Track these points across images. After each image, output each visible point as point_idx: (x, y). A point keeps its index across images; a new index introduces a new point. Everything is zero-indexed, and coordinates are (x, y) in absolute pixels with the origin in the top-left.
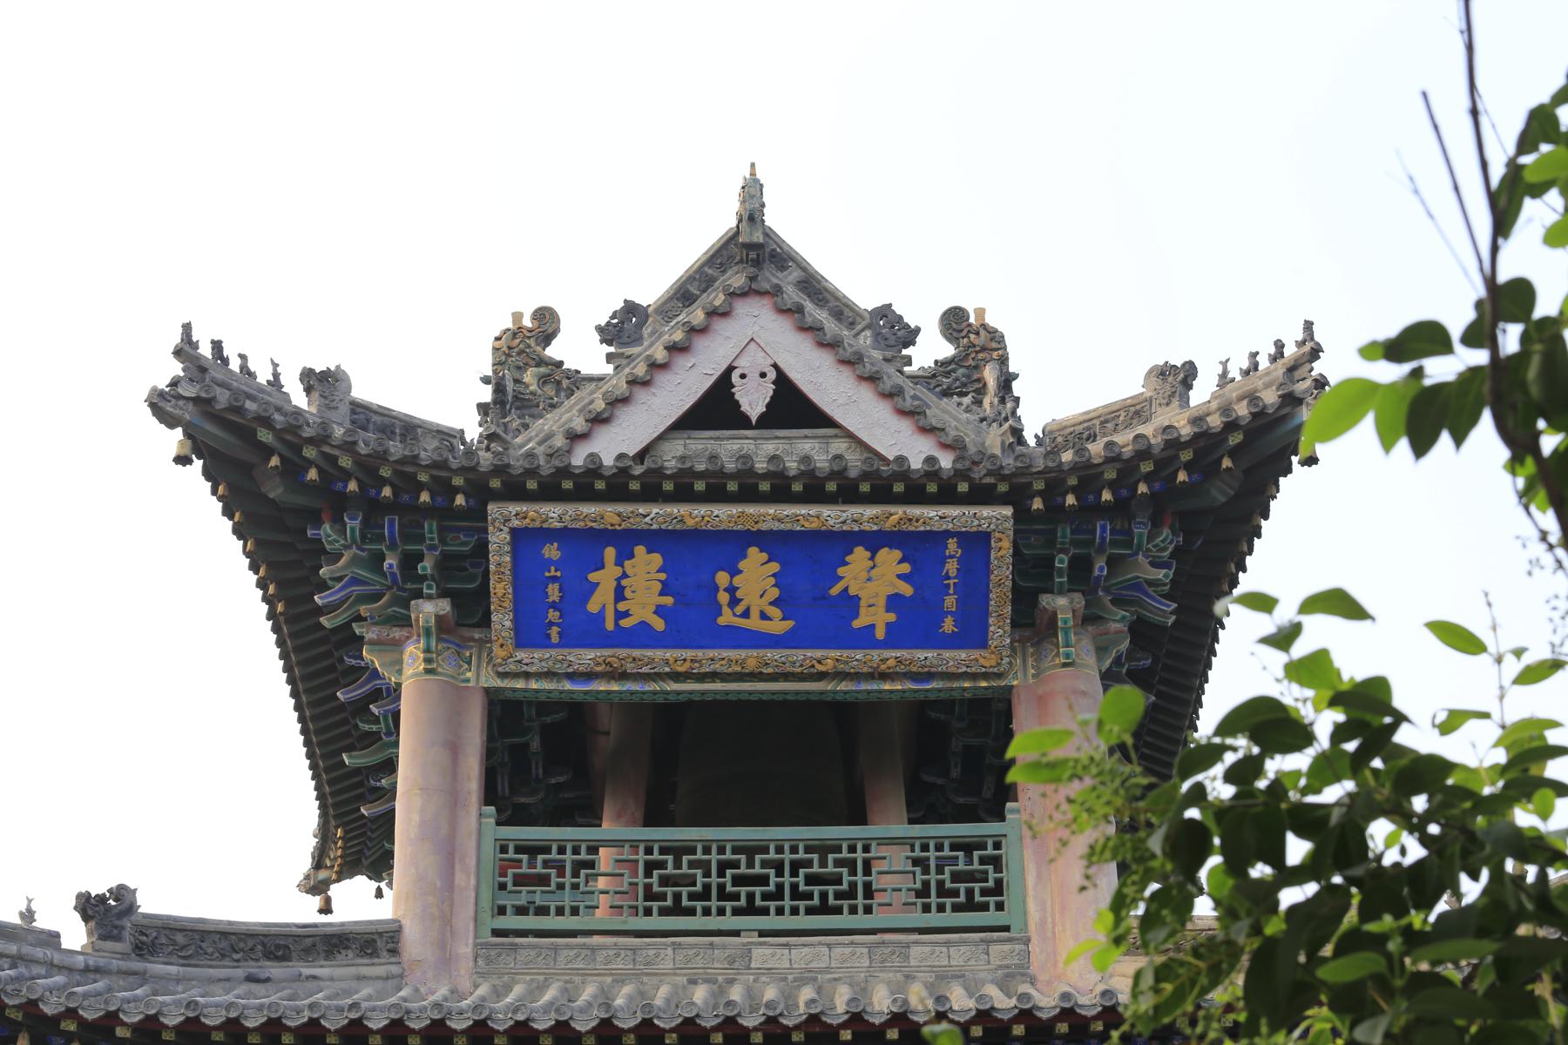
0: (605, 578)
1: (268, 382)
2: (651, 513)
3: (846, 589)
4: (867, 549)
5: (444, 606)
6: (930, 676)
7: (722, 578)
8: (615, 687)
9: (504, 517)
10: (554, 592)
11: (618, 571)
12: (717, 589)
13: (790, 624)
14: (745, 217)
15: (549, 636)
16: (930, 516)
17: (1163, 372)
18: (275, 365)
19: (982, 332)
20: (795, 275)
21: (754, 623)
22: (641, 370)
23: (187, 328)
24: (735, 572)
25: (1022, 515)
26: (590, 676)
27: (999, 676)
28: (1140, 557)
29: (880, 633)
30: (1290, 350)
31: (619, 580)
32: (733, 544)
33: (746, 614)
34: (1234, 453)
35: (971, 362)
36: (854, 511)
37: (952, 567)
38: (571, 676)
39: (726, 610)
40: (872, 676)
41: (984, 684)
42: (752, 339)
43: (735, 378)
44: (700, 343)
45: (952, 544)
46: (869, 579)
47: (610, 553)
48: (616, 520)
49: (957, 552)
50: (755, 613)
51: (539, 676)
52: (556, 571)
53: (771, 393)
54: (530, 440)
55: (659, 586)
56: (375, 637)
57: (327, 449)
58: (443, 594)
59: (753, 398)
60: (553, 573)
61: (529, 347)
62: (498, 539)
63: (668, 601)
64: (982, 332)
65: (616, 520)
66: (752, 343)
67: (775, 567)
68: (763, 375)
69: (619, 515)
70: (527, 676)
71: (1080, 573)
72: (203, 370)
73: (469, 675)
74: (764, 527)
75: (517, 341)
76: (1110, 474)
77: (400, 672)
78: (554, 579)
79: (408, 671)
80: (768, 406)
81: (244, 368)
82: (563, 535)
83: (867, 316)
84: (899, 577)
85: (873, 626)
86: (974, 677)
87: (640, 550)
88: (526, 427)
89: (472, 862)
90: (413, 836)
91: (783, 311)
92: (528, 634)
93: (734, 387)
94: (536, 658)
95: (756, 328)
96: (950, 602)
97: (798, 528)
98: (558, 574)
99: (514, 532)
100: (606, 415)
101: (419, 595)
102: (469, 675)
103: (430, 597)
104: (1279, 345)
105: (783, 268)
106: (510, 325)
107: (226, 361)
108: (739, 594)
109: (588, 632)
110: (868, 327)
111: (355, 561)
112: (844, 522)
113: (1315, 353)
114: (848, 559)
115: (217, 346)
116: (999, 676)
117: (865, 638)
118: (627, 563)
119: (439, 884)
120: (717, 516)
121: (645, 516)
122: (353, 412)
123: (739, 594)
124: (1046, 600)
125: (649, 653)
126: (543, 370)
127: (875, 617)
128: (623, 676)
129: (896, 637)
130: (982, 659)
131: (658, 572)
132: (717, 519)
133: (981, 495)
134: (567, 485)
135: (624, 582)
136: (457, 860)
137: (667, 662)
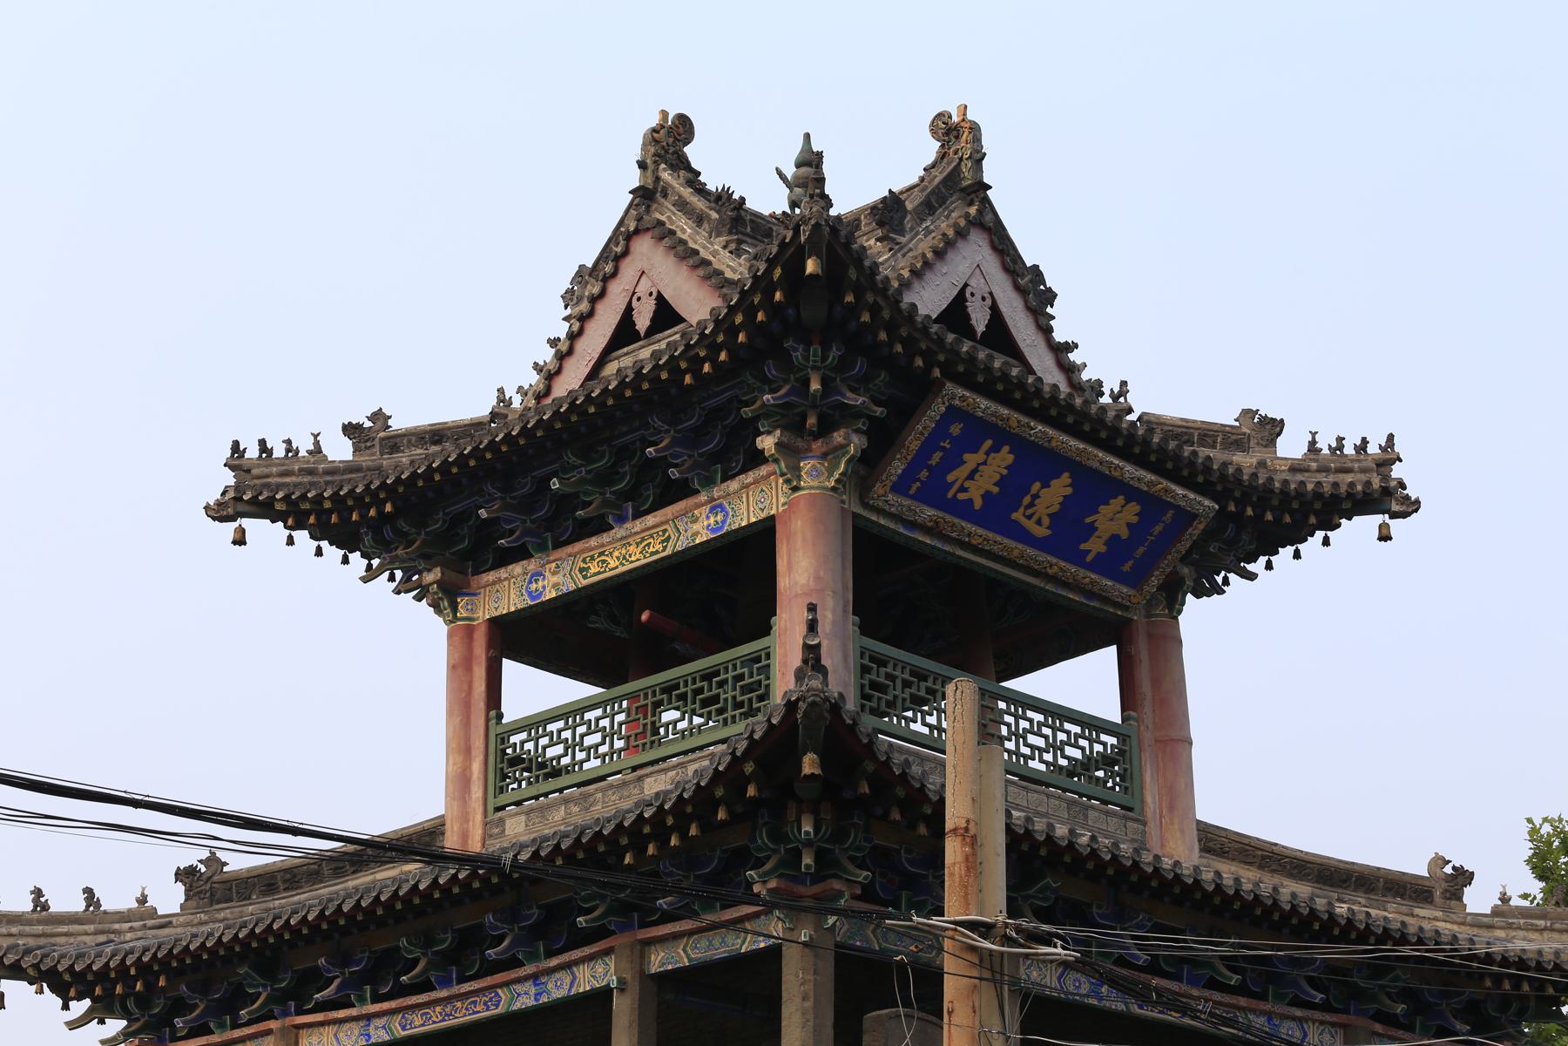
0: (971, 460)
7: (1037, 485)
12: (1027, 491)
21: (1030, 525)
24: (1046, 485)
27: (1126, 608)
29: (1089, 558)
31: (979, 465)
36: (1141, 473)
43: (968, 295)
46: (1112, 520)
50: (1035, 518)
53: (989, 317)
55: (997, 477)
59: (979, 319)
62: (938, 408)
63: (996, 490)
69: (1019, 422)
80: (986, 326)
87: (1006, 448)
96: (1141, 550)
99: (951, 408)
108: (1037, 502)
109: (935, 494)
112: (1133, 478)
127: (1095, 546)
129: (1104, 564)
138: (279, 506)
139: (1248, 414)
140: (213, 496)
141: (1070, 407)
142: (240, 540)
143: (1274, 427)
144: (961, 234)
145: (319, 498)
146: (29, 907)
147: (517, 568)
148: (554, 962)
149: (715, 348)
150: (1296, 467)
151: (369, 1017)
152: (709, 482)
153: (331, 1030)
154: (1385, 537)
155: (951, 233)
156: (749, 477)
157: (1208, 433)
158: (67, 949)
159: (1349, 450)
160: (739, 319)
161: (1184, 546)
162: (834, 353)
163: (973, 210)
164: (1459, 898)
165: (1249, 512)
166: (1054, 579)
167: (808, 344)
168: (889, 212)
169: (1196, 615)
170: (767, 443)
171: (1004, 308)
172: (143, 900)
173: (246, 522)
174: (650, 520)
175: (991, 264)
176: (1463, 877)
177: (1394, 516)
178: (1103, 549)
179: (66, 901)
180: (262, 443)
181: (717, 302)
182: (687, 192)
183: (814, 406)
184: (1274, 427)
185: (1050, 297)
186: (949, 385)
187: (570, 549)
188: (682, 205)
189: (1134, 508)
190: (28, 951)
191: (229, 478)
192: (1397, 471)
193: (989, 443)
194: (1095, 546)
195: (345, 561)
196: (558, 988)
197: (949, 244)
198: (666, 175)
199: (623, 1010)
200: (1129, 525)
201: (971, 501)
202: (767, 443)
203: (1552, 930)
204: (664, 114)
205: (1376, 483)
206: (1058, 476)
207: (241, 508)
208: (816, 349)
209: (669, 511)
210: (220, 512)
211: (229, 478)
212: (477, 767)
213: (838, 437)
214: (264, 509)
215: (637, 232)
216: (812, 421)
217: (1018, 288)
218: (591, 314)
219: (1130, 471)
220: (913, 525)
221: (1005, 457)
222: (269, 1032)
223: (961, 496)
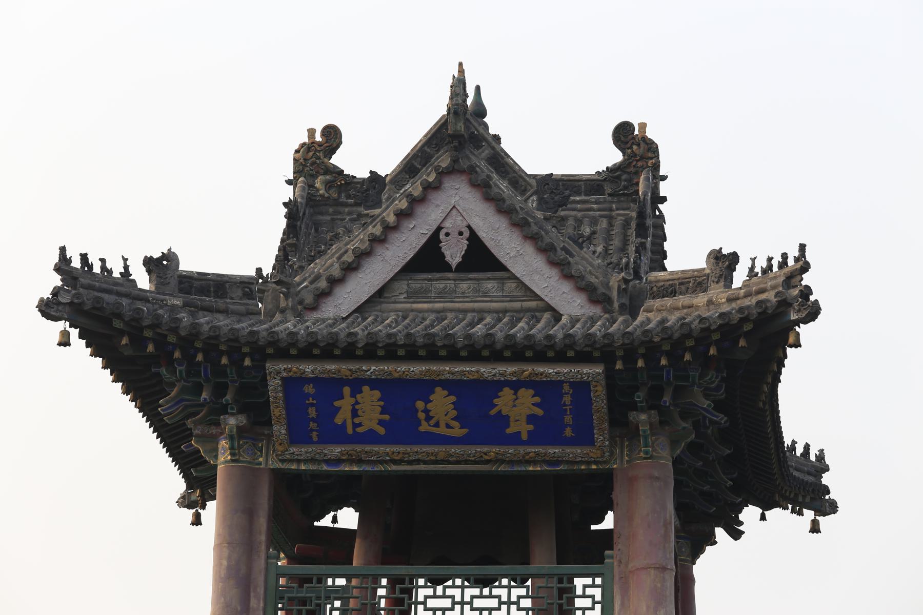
1: (121, 273)
2: (370, 369)
3: (500, 411)
4: (511, 389)
5: (242, 420)
6: (557, 462)
9: (277, 370)
10: (312, 412)
11: (352, 400)
13: (465, 431)
14: (452, 111)
15: (311, 438)
16: (550, 370)
17: (716, 256)
18: (125, 260)
19: (642, 144)
20: (486, 152)
21: (442, 430)
22: (377, 230)
23: (63, 250)
24: (427, 401)
25: (610, 374)
26: (338, 461)
27: (605, 462)
28: (696, 388)
29: (524, 436)
32: (425, 387)
33: (437, 425)
34: (747, 335)
35: (632, 169)
37: (567, 399)
38: (328, 462)
39: (424, 423)
40: (519, 462)
41: (594, 467)
42: (454, 207)
43: (442, 236)
44: (420, 210)
45: (566, 387)
46: (515, 406)
47: (347, 390)
48: (348, 373)
49: (570, 391)
50: (442, 424)
51: (306, 461)
52: (313, 400)
53: (465, 248)
54: (304, 280)
56: (200, 433)
57: (159, 331)
58: (240, 412)
60: (311, 401)
61: (319, 158)
64: (642, 144)
65: (348, 373)
66: (454, 211)
67: (453, 398)
68: (461, 234)
69: (350, 370)
70: (299, 461)
71: (653, 403)
72: (75, 279)
73: (261, 459)
74: (443, 378)
75: (311, 154)
76: (666, 347)
77: (216, 457)
78: (312, 405)
79: (221, 459)
80: (463, 257)
81: (104, 268)
82: (316, 381)
83: (534, 183)
84: (533, 404)
85: (520, 432)
86: (588, 463)
87: (366, 389)
88: (302, 268)
89: (261, 591)
90: (223, 576)
91: (474, 185)
92: (297, 436)
93: (441, 242)
94: (302, 451)
95: (457, 198)
96: (568, 419)
97: (465, 379)
98: (315, 402)
100: (354, 265)
101: (225, 412)
102: (261, 459)
103: (233, 414)
104: (785, 256)
105: (479, 147)
106: (306, 140)
107: (91, 267)
108: (431, 414)
110: (535, 193)
111: (183, 390)
113: (806, 267)
114: (500, 394)
115: (84, 257)
116: (605, 462)
117: (515, 439)
118: (358, 396)
119: (239, 609)
120: (413, 371)
121: (367, 371)
122: (180, 282)
123: (431, 414)
124: (632, 415)
125: (376, 448)
126: (328, 177)
128: (360, 461)
129: (534, 439)
130: (592, 452)
131: (378, 401)
132: (413, 373)
133: (584, 357)
134: (316, 351)
135: (357, 407)
136: (252, 590)
137: (387, 454)
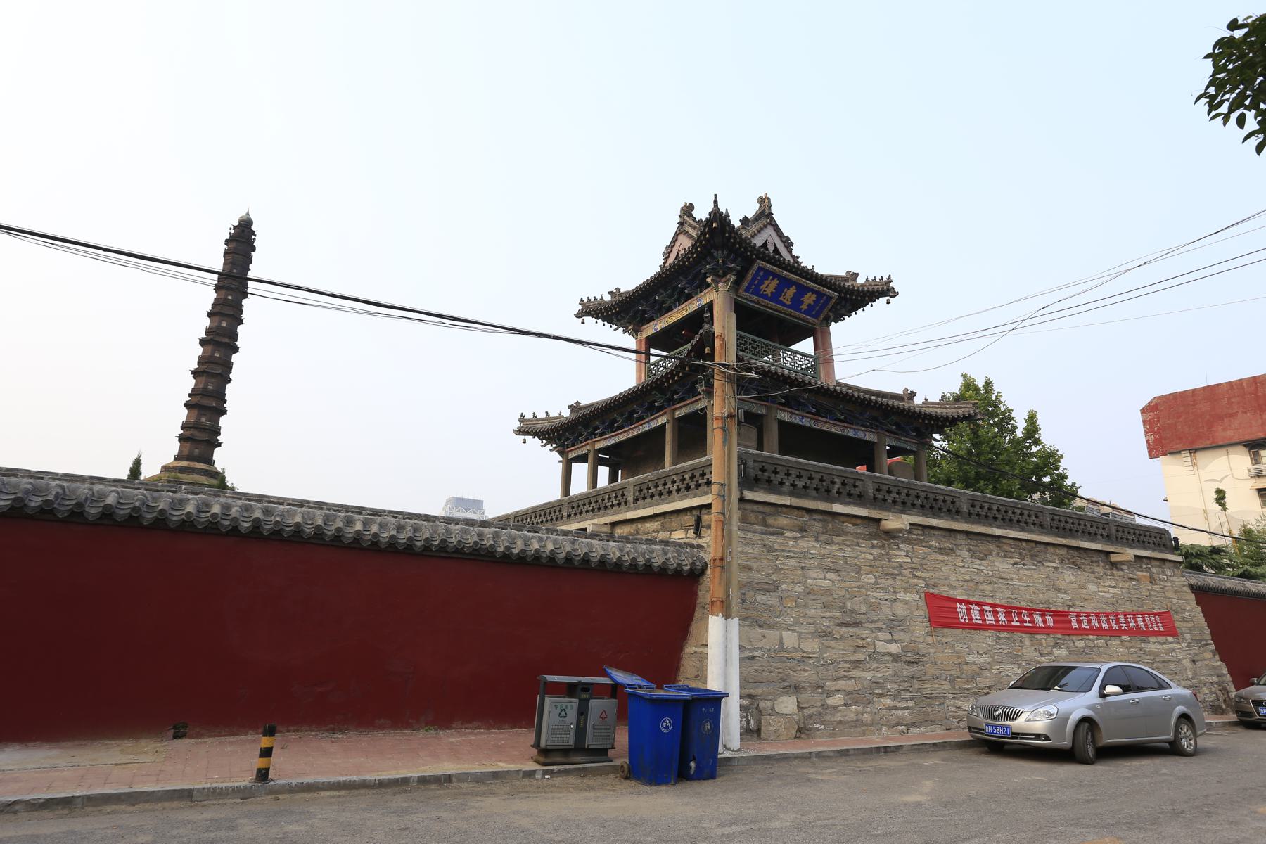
0: (767, 282)
7: (786, 290)
8: (756, 305)
12: (783, 291)
21: (785, 301)
24: (788, 289)
30: (885, 279)
36: (816, 285)
45: (825, 297)
59: (771, 249)
62: (755, 267)
63: (774, 291)
94: (746, 294)
99: (759, 267)
127: (804, 307)
129: (806, 312)
133: (835, 290)
138: (592, 313)
139: (849, 272)
140: (576, 312)
141: (794, 266)
142: (583, 322)
143: (856, 275)
144: (765, 226)
145: (601, 309)
146: (532, 417)
147: (651, 323)
148: (652, 417)
149: (693, 254)
150: (862, 285)
151: (610, 437)
152: (696, 294)
153: (602, 442)
154: (888, 303)
155: (762, 226)
156: (707, 290)
157: (837, 278)
158: (539, 426)
159: (878, 280)
160: (698, 244)
161: (830, 306)
162: (725, 253)
163: (769, 220)
164: (913, 400)
165: (848, 296)
166: (791, 316)
167: (718, 251)
168: (745, 221)
169: (835, 328)
170: (709, 280)
171: (778, 246)
172: (560, 414)
173: (584, 318)
174: (683, 306)
175: (774, 235)
176: (913, 394)
177: (891, 297)
178: (806, 308)
179: (541, 415)
180: (588, 298)
181: (691, 241)
182: (691, 222)
183: (721, 269)
184: (856, 275)
185: (792, 244)
186: (758, 261)
187: (664, 316)
188: (690, 225)
189: (814, 296)
190: (530, 428)
191: (580, 307)
192: (892, 285)
193: (771, 277)
194: (804, 307)
195: (611, 327)
196: (654, 424)
197: (762, 229)
198: (686, 218)
199: (669, 428)
200: (814, 301)
201: (767, 294)
202: (709, 280)
203: (941, 408)
204: (686, 203)
205: (885, 288)
206: (792, 287)
207: (584, 314)
208: (720, 252)
209: (687, 303)
210: (578, 316)
211: (580, 307)
212: (643, 375)
213: (728, 277)
214: (588, 314)
215: (679, 234)
216: (721, 272)
217: (782, 241)
218: (669, 256)
219: (812, 285)
220: (751, 301)
221: (776, 281)
222: (588, 444)
223: (765, 293)
